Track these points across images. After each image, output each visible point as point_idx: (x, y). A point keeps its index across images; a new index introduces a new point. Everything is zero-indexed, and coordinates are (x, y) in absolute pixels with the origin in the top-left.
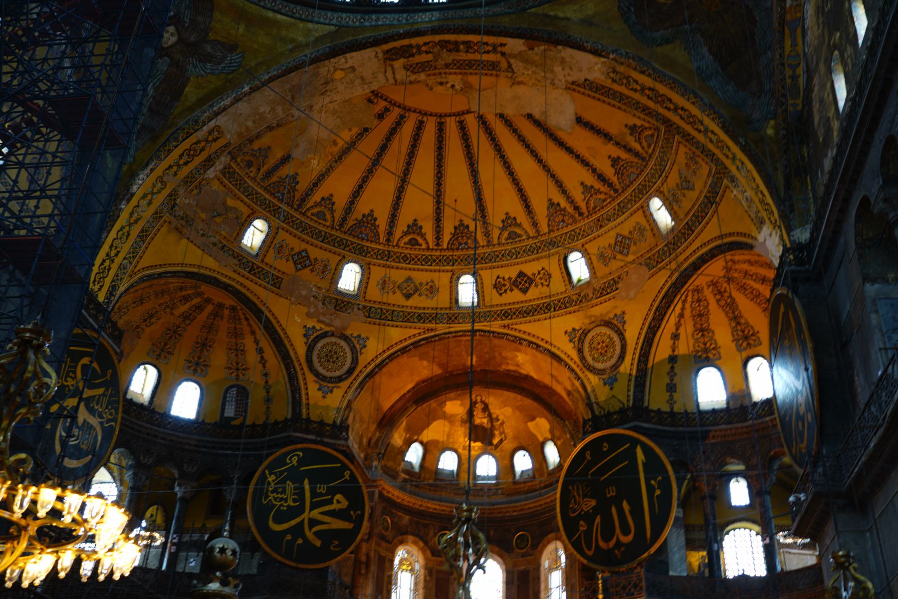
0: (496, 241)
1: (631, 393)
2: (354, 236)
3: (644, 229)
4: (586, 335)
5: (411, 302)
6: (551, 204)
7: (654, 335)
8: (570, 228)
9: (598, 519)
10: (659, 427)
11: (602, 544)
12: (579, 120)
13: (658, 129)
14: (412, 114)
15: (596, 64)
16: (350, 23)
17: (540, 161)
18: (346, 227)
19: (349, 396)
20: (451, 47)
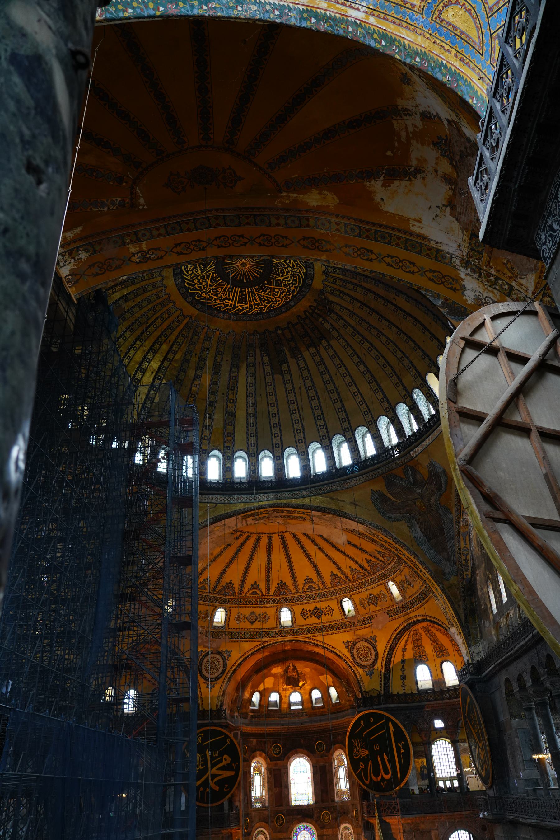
0: (301, 591)
1: (382, 683)
2: (221, 595)
3: (386, 595)
4: (355, 645)
5: (254, 626)
6: (332, 574)
7: (393, 651)
8: (343, 586)
9: (370, 763)
10: (399, 705)
11: (373, 778)
12: (349, 543)
17: (326, 555)
18: (217, 591)
19: (223, 688)
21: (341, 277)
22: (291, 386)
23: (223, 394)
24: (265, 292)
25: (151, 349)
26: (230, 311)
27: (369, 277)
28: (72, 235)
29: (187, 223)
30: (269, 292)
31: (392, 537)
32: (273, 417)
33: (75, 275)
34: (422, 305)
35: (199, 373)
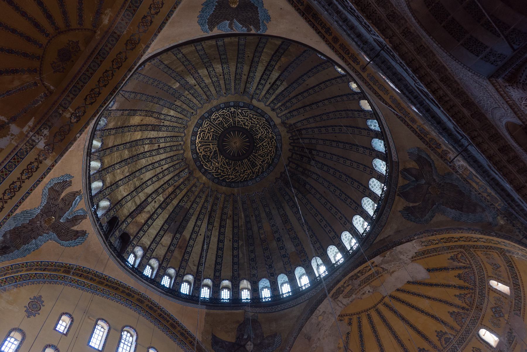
0: (442, 348)
6: (451, 314)
13: (461, 252)
14: (362, 314)
15: (413, 244)
16: (312, 295)
17: (429, 298)
20: (355, 277)
21: (280, 104)
22: (319, 195)
23: (283, 229)
24: (260, 150)
25: (221, 226)
26: (253, 176)
27: (287, 87)
28: (32, 123)
29: (78, 83)
30: (262, 149)
31: (435, 231)
32: (321, 222)
33: (50, 145)
34: (313, 69)
35: (260, 225)
